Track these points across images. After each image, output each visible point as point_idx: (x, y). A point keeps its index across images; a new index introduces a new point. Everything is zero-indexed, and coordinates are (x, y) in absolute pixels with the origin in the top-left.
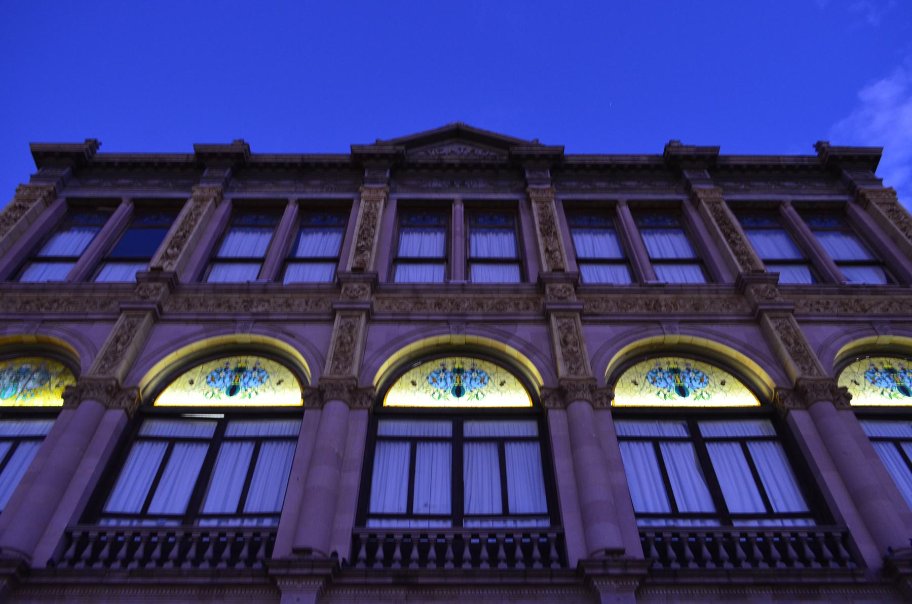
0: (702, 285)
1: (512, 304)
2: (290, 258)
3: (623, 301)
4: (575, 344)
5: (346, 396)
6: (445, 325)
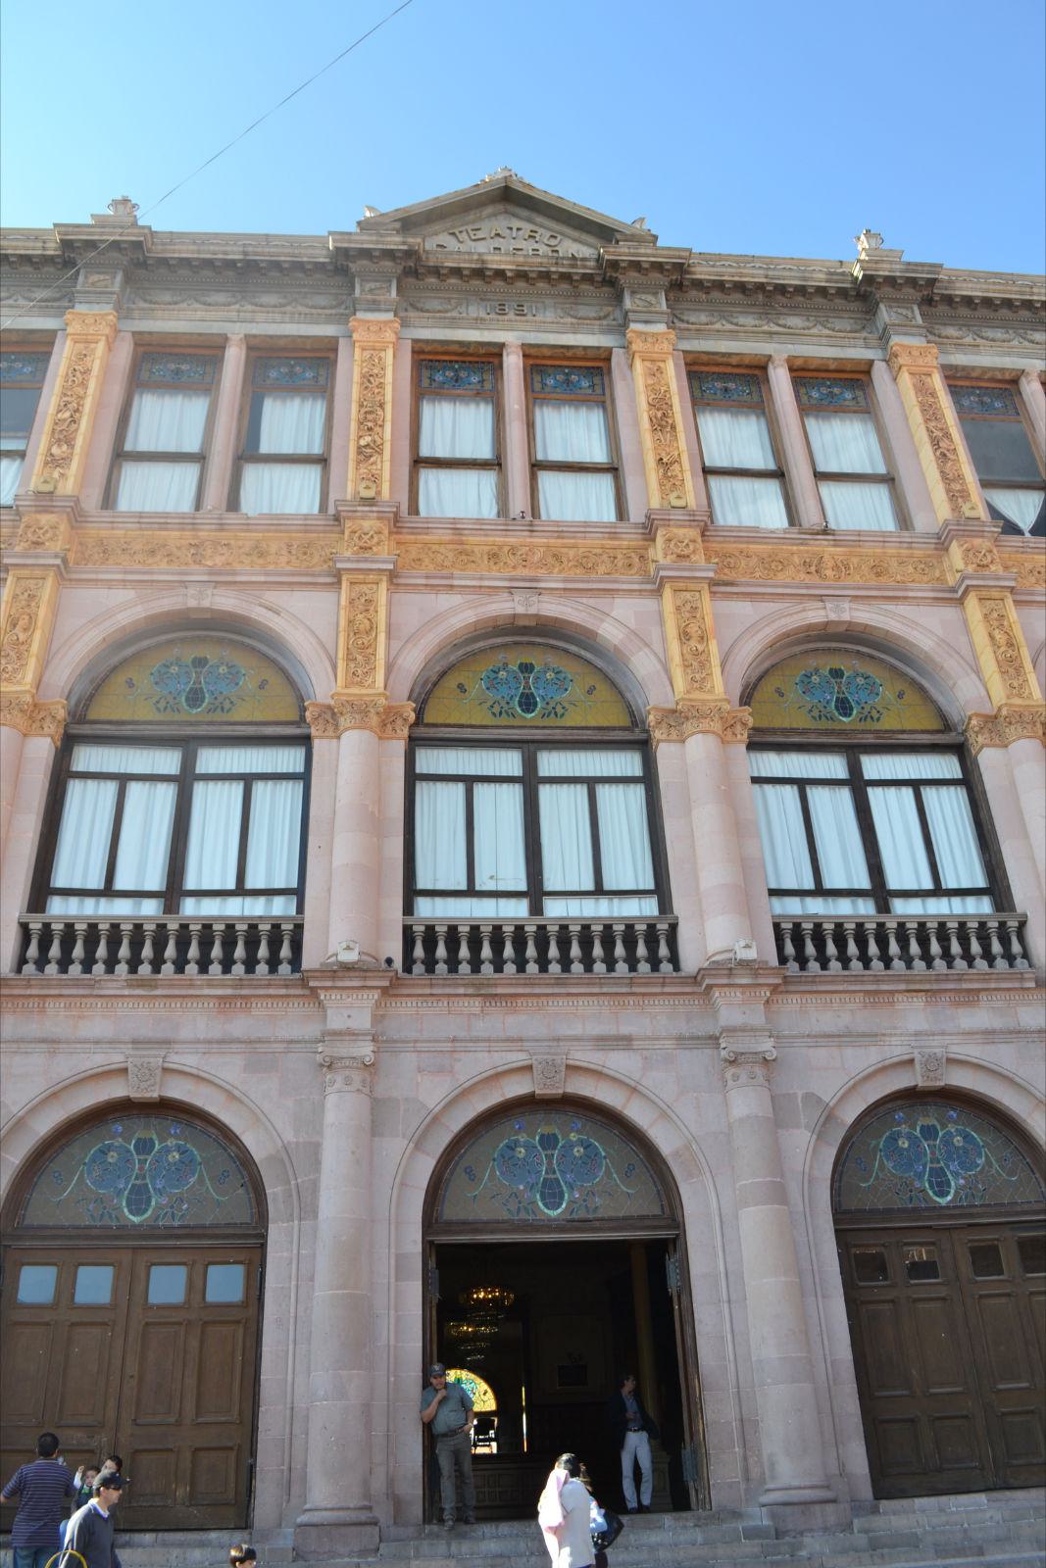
1: (605, 557)
2: (248, 452)
5: (374, 720)
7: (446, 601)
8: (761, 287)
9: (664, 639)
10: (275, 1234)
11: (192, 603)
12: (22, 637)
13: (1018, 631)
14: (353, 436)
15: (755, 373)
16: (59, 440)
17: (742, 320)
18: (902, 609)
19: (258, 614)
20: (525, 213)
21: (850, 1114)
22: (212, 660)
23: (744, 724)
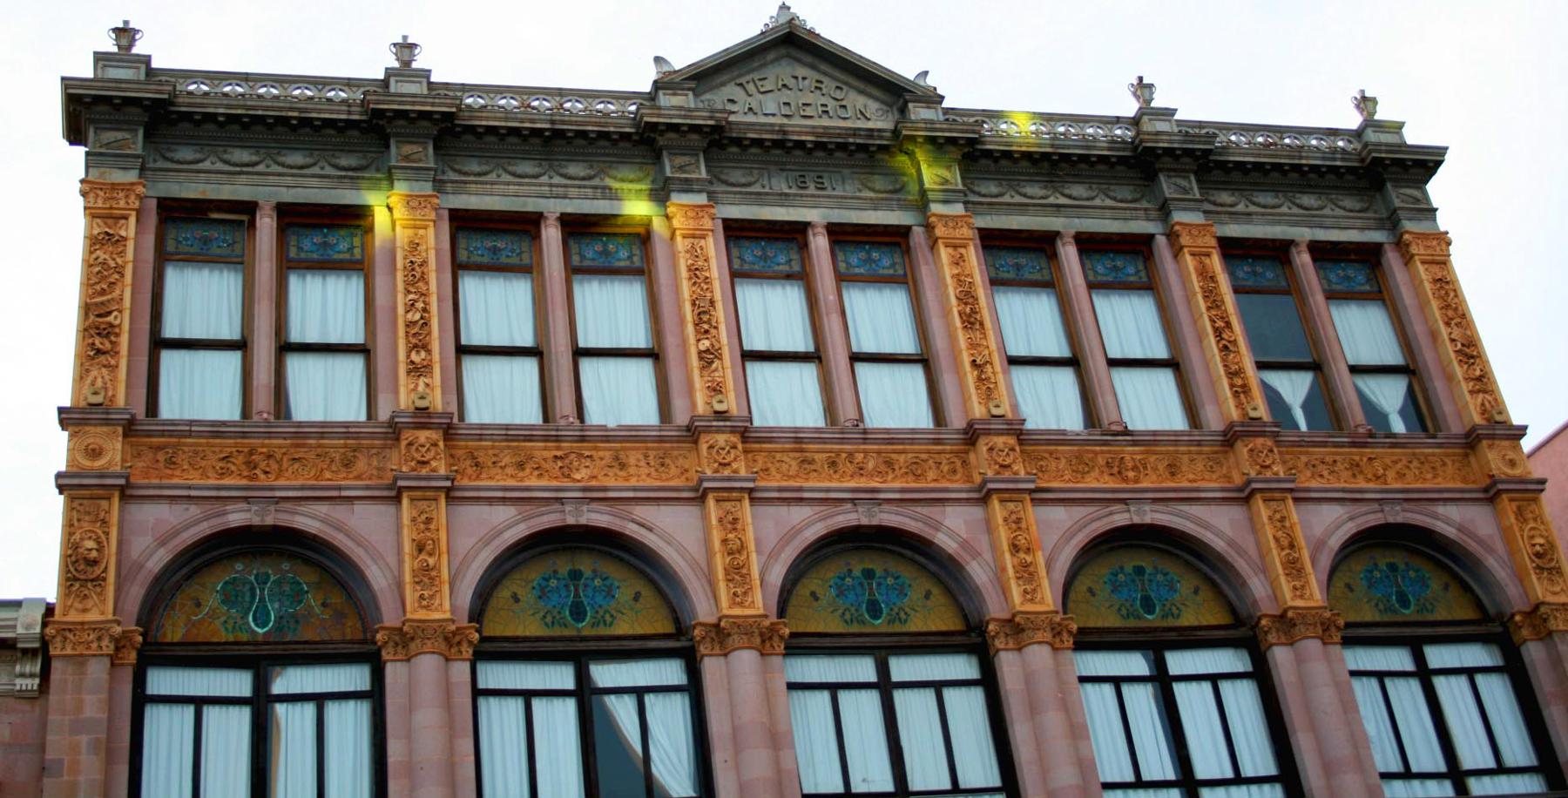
0: (1181, 433)
3: (1079, 457)
6: (849, 506)
7: (799, 514)
9: (994, 547)
11: (571, 521)
12: (431, 561)
13: (1301, 541)
14: (692, 340)
16: (415, 346)
19: (631, 529)
20: (809, 59)
22: (588, 573)
23: (1070, 632)
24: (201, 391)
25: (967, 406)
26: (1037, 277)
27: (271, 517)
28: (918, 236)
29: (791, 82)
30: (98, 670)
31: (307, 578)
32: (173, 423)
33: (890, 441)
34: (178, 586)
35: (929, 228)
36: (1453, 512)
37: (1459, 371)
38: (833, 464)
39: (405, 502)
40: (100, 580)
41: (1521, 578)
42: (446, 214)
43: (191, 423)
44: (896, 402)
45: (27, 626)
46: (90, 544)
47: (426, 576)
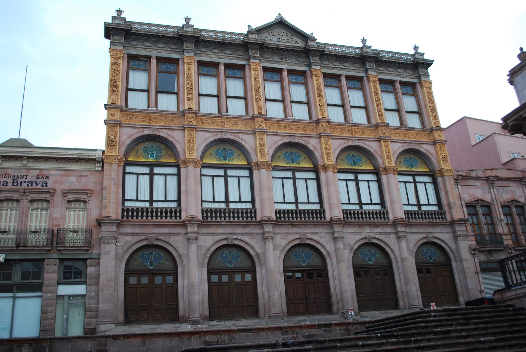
4: (329, 150)
7: (277, 138)
8: (340, 56)
9: (321, 148)
10: (258, 269)
11: (224, 137)
12: (192, 145)
14: (254, 96)
15: (338, 77)
17: (335, 64)
18: (367, 142)
19: (238, 140)
20: (285, 28)
21: (355, 247)
22: (227, 149)
24: (138, 101)
25: (317, 115)
26: (335, 85)
27: (155, 133)
28: (308, 73)
29: (280, 33)
30: (115, 166)
31: (163, 147)
32: (131, 109)
33: (299, 122)
34: (133, 147)
35: (311, 72)
36: (425, 146)
37: (431, 114)
38: (285, 127)
39: (186, 130)
40: (115, 146)
41: (439, 162)
42: (197, 61)
43: (136, 109)
44: (300, 113)
45: (98, 155)
46: (113, 137)
47: (190, 148)
